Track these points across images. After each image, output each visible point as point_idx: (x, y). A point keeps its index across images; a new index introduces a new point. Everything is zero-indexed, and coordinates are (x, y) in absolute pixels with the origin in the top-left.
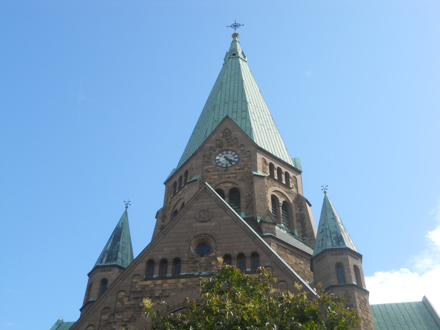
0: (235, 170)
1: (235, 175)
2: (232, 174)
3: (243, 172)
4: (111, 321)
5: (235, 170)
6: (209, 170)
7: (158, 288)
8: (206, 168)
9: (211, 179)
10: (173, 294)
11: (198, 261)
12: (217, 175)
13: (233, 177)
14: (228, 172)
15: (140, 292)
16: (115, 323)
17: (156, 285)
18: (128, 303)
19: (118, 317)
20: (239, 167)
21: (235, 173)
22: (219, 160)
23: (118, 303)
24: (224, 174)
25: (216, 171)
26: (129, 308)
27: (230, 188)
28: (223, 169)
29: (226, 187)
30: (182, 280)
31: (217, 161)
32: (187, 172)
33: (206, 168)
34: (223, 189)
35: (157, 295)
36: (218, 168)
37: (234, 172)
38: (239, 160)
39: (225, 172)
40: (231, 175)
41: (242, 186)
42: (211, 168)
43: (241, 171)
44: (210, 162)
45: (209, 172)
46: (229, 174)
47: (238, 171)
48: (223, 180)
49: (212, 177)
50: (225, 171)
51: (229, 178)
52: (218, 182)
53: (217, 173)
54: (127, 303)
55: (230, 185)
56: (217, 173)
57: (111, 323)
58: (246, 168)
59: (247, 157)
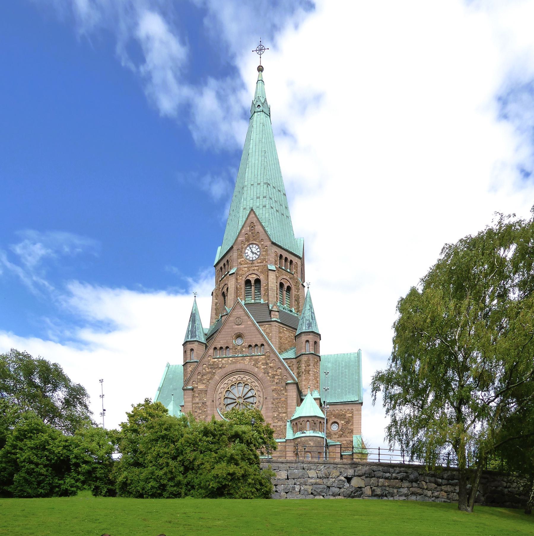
0: (258, 263)
1: (257, 268)
2: (256, 266)
4: (202, 379)
8: (239, 261)
9: (243, 271)
11: (237, 348)
13: (256, 269)
15: (213, 365)
16: (204, 380)
17: (219, 361)
18: (208, 370)
19: (205, 377)
20: (260, 261)
21: (258, 266)
22: (247, 253)
26: (209, 373)
30: (231, 359)
31: (246, 255)
33: (239, 261)
35: (220, 366)
36: (247, 261)
39: (251, 265)
40: (255, 268)
41: (262, 278)
42: (243, 261)
43: (261, 264)
46: (254, 267)
47: (259, 264)
49: (244, 269)
51: (254, 270)
52: (247, 274)
53: (246, 266)
55: (255, 276)
56: (246, 266)
58: (265, 262)
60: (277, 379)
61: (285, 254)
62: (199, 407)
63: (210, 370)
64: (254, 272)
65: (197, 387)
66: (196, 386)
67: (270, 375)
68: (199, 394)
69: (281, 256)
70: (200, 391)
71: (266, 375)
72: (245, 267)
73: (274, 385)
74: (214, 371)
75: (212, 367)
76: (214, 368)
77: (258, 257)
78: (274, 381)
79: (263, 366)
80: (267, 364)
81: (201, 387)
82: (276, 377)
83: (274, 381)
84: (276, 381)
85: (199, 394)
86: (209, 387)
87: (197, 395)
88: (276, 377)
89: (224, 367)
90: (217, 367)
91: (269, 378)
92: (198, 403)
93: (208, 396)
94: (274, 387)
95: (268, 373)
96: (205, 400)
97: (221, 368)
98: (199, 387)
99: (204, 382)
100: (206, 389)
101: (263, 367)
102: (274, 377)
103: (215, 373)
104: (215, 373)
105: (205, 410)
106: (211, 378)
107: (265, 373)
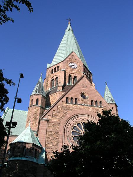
7: (71, 107)
17: (70, 106)
26: (62, 112)
30: (79, 106)
32: (58, 67)
33: (66, 67)
55: (74, 75)
57: (56, 116)
62: (52, 135)
65: (52, 120)
66: (51, 119)
74: (66, 111)
75: (65, 108)
76: (67, 110)
81: (55, 120)
86: (62, 121)
92: (51, 132)
93: (60, 128)
96: (57, 130)
98: (53, 120)
103: (67, 112)
104: (67, 112)
105: (57, 138)
106: (63, 116)
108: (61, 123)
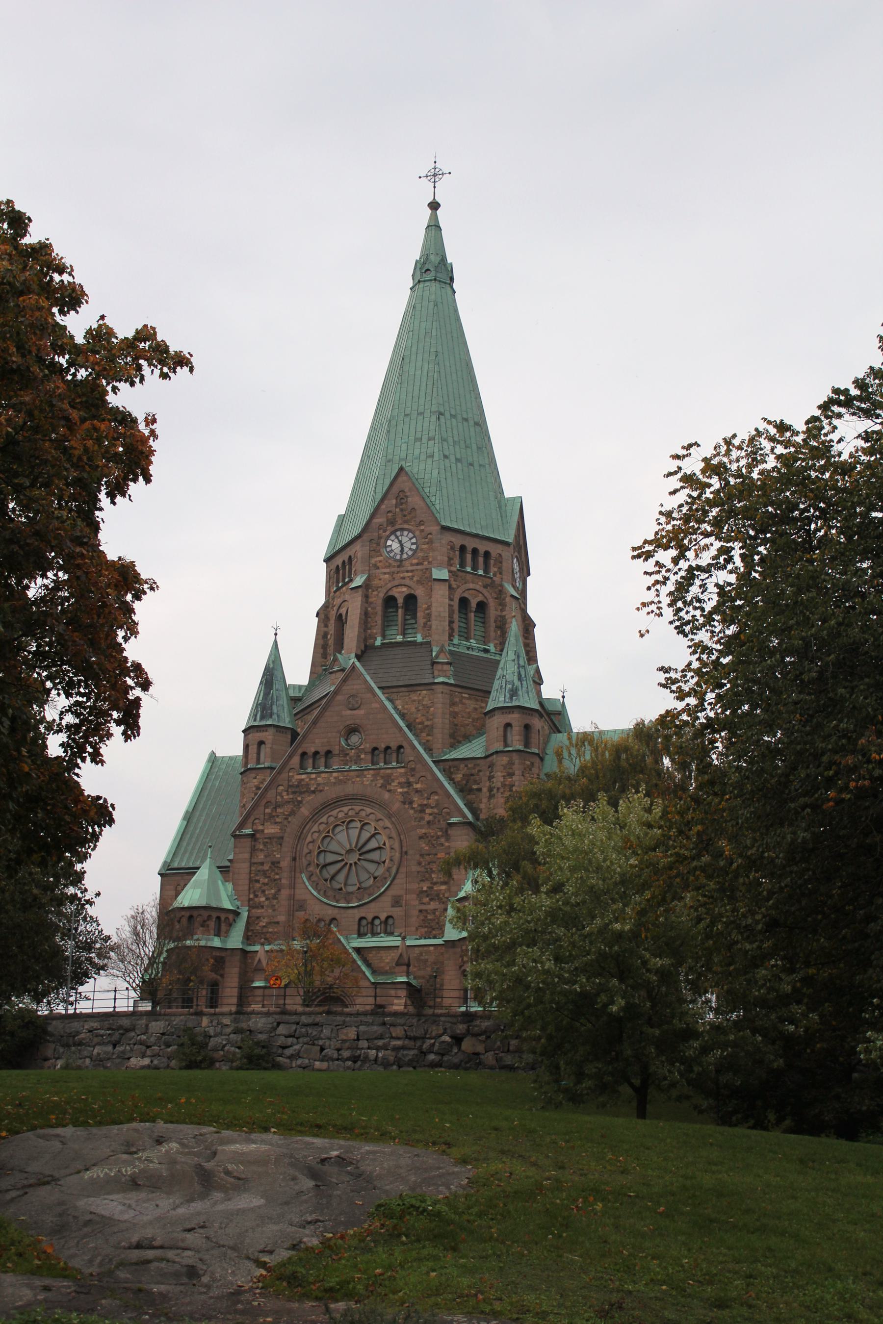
0: (412, 565)
1: (410, 574)
2: (407, 571)
3: (422, 570)
5: (412, 565)
6: (379, 564)
8: (373, 561)
10: (326, 788)
12: (388, 573)
14: (402, 569)
16: (278, 816)
19: (279, 810)
21: (412, 571)
22: (391, 546)
23: (278, 797)
24: (398, 572)
25: (386, 567)
26: (289, 802)
27: (404, 595)
28: (396, 564)
29: (399, 592)
31: (388, 549)
33: (373, 561)
34: (396, 595)
35: (312, 789)
37: (410, 568)
38: (417, 548)
40: (407, 574)
42: (380, 561)
43: (419, 567)
44: (379, 551)
45: (378, 568)
46: (403, 572)
48: (396, 583)
49: (382, 576)
50: (399, 567)
51: (403, 578)
52: (390, 586)
53: (387, 570)
54: (286, 797)
55: (404, 589)
56: (387, 570)
58: (426, 563)
59: (428, 543)
60: (430, 814)
61: (470, 544)
63: (291, 796)
64: (403, 582)
65: (263, 831)
66: (261, 827)
67: (415, 805)
68: (265, 846)
69: (463, 548)
70: (269, 838)
71: (407, 806)
72: (385, 573)
73: (421, 827)
75: (297, 790)
76: (301, 793)
77: (413, 555)
78: (422, 818)
79: (402, 787)
80: (409, 784)
81: (271, 829)
82: (428, 811)
83: (422, 818)
84: (428, 818)
85: (265, 844)
86: (288, 830)
87: (261, 847)
88: (428, 811)
89: (321, 791)
90: (307, 791)
91: (412, 812)
94: (424, 831)
95: (411, 803)
97: (314, 792)
98: (266, 831)
99: (278, 820)
100: (281, 835)
101: (400, 790)
102: (422, 811)
103: (301, 802)
104: (301, 802)
106: (293, 813)
107: (404, 803)
108: (286, 835)
